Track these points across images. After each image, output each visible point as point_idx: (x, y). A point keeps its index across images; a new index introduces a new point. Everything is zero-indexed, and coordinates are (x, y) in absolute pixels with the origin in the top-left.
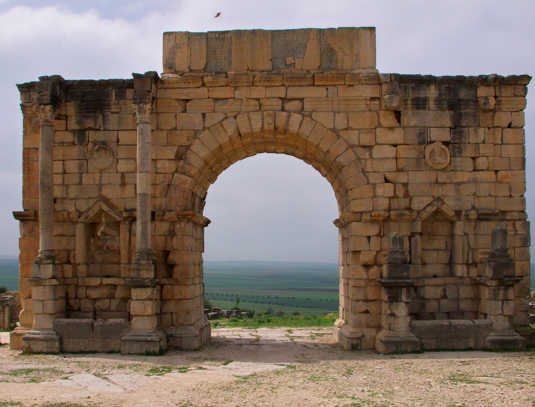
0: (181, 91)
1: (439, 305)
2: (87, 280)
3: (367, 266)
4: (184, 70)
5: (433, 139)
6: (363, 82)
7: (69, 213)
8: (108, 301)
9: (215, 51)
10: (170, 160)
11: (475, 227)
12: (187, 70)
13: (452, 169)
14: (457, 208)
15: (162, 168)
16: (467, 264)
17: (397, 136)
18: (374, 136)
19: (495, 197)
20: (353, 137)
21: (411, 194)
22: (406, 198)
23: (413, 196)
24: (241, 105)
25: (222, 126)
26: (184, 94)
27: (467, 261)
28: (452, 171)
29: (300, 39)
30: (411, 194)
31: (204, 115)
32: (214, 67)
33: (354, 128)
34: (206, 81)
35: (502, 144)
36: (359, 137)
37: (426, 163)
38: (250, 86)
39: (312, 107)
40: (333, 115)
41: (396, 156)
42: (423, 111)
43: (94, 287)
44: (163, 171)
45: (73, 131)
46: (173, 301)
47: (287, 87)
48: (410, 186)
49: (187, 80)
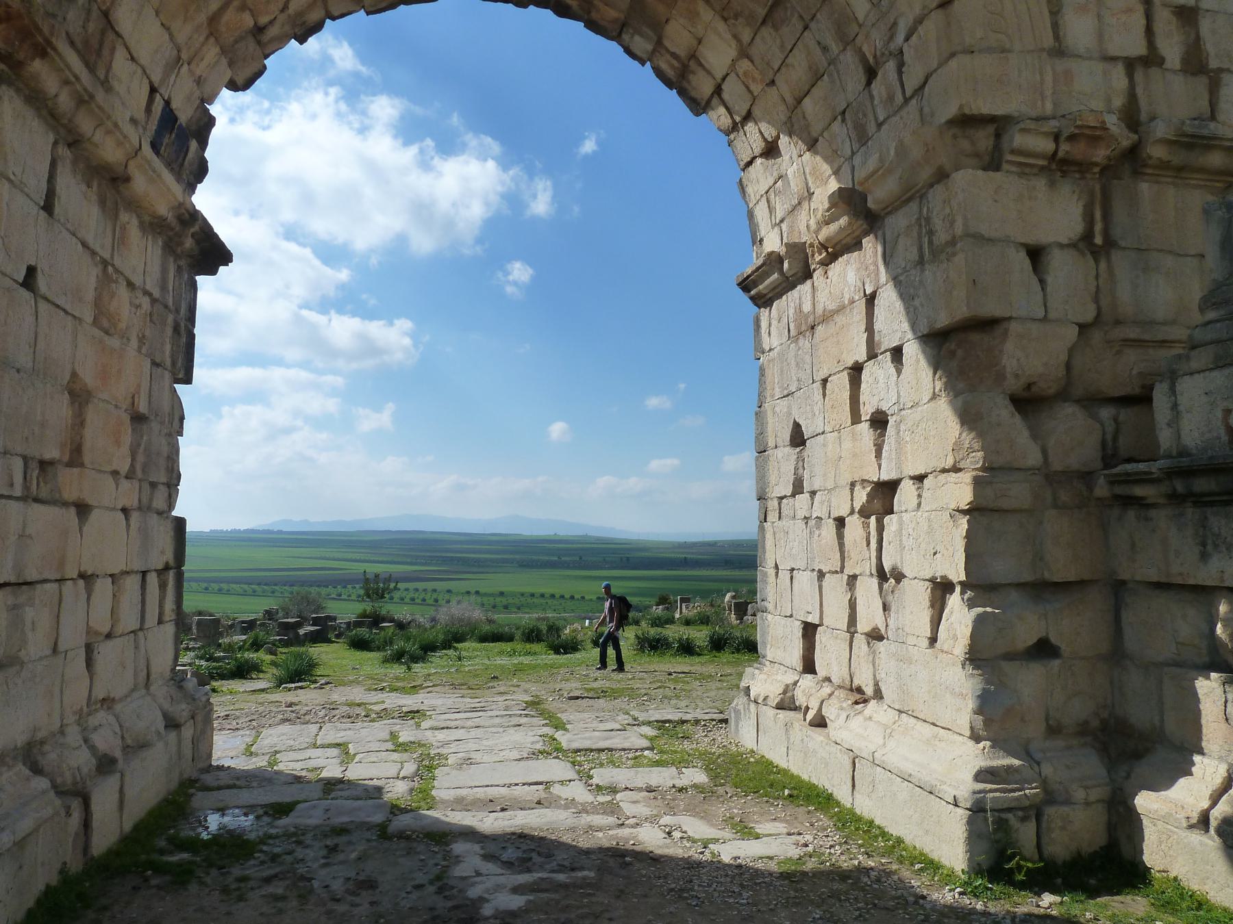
22: (1194, 74)
23: (1221, 70)
30: (1213, 64)
48: (1205, 26)
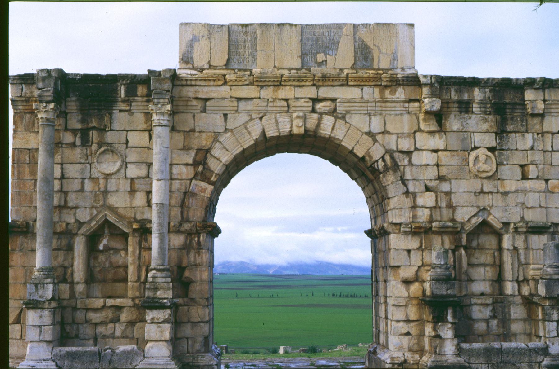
0: (200, 89)
1: (488, 326)
2: (88, 301)
3: (407, 282)
4: (204, 66)
5: (477, 145)
6: (401, 83)
7: (68, 224)
8: (111, 325)
9: (238, 46)
10: (187, 165)
11: (526, 240)
12: (206, 66)
13: (499, 177)
14: (505, 220)
15: (178, 174)
16: (518, 282)
17: (438, 142)
18: (413, 141)
19: (546, 208)
20: (392, 142)
21: (454, 205)
23: (457, 206)
24: (267, 105)
25: (246, 128)
26: (203, 92)
27: (518, 277)
28: (499, 179)
29: (332, 34)
31: (225, 115)
32: (237, 63)
33: (391, 131)
34: (228, 79)
35: (553, 151)
36: (397, 141)
37: (470, 171)
38: (277, 85)
39: (346, 108)
40: (368, 118)
41: (438, 163)
42: (466, 115)
43: (96, 310)
44: (179, 177)
45: (74, 132)
46: (189, 324)
47: (318, 87)
48: (453, 195)
49: (208, 77)
